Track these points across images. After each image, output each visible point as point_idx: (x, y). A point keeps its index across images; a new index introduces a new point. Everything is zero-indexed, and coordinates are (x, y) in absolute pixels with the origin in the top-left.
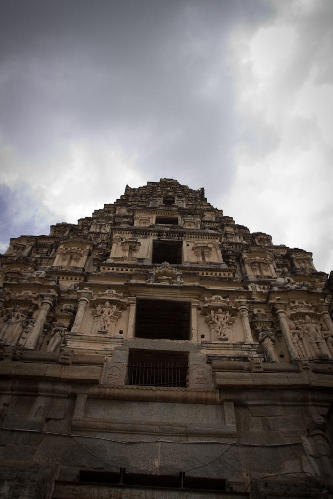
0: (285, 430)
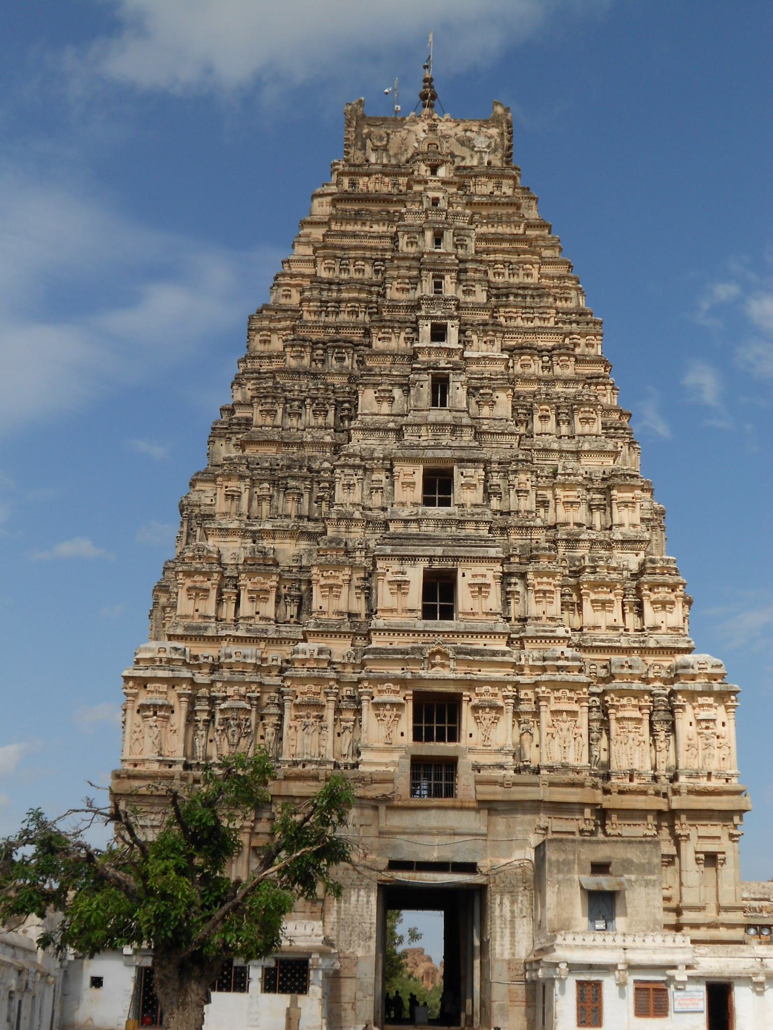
0: (519, 828)
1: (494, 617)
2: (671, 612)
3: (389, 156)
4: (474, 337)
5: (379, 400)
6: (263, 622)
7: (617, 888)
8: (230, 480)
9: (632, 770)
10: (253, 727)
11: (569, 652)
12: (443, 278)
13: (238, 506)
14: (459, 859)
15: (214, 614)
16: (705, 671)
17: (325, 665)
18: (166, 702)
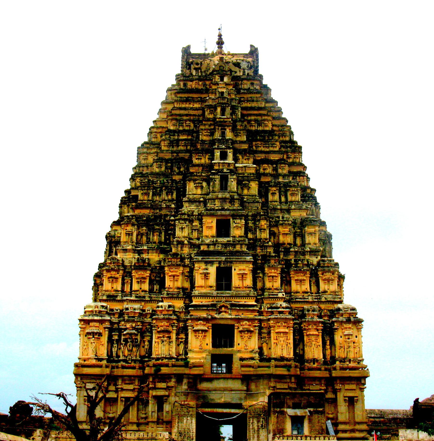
0: (262, 387)
1: (249, 289)
2: (332, 284)
3: (201, 72)
4: (240, 157)
5: (196, 187)
6: (143, 293)
7: (304, 415)
8: (127, 226)
9: (314, 359)
10: (139, 342)
11: (284, 305)
12: (226, 130)
13: (132, 239)
14: (234, 402)
15: (120, 289)
16: (347, 312)
17: (171, 313)
18: (98, 331)
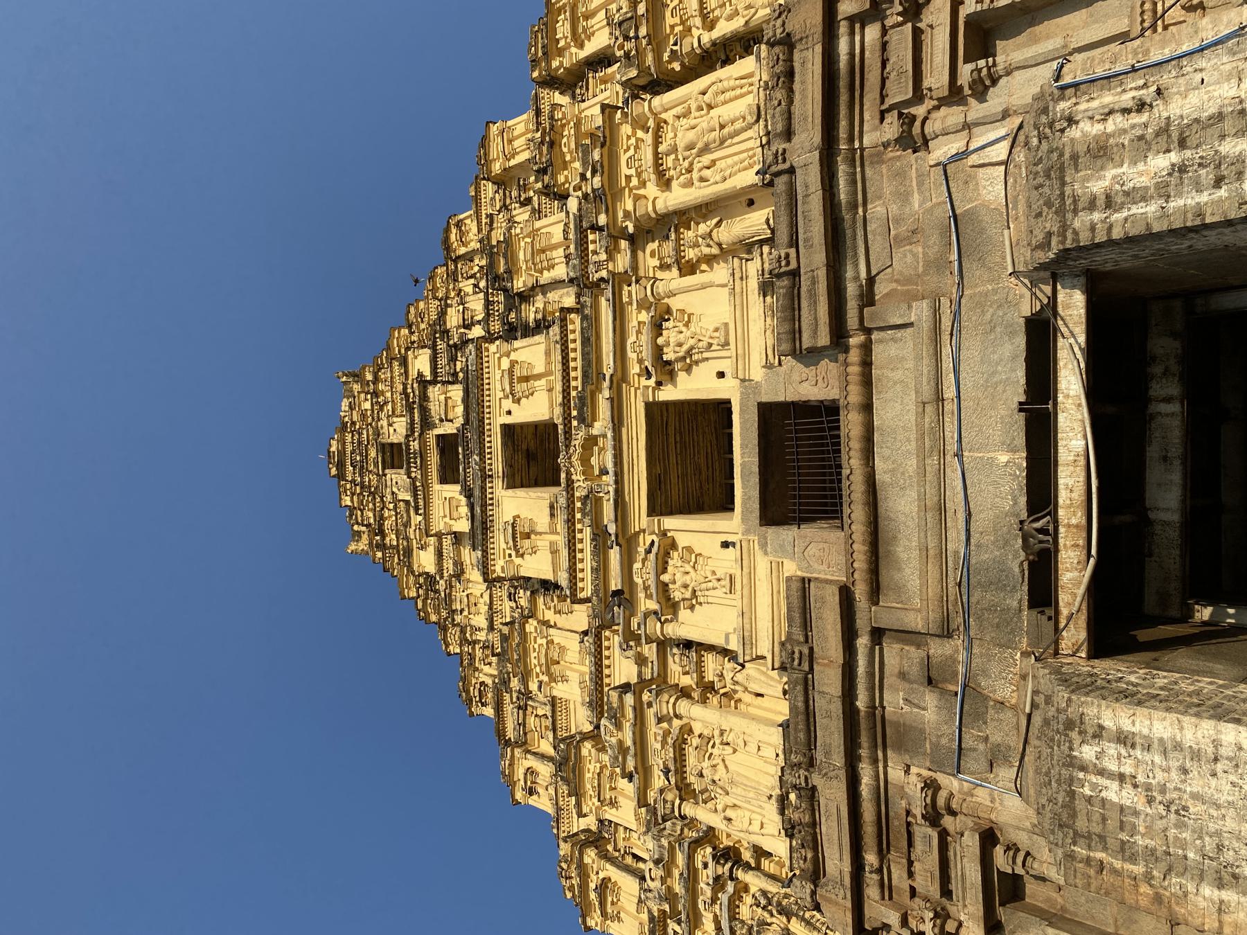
0: (916, 199)
